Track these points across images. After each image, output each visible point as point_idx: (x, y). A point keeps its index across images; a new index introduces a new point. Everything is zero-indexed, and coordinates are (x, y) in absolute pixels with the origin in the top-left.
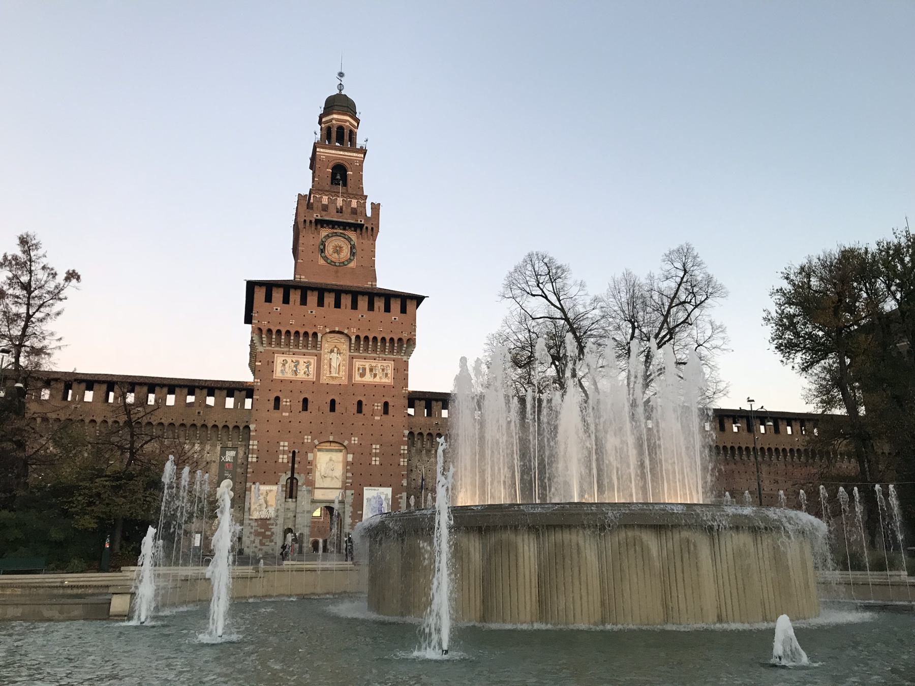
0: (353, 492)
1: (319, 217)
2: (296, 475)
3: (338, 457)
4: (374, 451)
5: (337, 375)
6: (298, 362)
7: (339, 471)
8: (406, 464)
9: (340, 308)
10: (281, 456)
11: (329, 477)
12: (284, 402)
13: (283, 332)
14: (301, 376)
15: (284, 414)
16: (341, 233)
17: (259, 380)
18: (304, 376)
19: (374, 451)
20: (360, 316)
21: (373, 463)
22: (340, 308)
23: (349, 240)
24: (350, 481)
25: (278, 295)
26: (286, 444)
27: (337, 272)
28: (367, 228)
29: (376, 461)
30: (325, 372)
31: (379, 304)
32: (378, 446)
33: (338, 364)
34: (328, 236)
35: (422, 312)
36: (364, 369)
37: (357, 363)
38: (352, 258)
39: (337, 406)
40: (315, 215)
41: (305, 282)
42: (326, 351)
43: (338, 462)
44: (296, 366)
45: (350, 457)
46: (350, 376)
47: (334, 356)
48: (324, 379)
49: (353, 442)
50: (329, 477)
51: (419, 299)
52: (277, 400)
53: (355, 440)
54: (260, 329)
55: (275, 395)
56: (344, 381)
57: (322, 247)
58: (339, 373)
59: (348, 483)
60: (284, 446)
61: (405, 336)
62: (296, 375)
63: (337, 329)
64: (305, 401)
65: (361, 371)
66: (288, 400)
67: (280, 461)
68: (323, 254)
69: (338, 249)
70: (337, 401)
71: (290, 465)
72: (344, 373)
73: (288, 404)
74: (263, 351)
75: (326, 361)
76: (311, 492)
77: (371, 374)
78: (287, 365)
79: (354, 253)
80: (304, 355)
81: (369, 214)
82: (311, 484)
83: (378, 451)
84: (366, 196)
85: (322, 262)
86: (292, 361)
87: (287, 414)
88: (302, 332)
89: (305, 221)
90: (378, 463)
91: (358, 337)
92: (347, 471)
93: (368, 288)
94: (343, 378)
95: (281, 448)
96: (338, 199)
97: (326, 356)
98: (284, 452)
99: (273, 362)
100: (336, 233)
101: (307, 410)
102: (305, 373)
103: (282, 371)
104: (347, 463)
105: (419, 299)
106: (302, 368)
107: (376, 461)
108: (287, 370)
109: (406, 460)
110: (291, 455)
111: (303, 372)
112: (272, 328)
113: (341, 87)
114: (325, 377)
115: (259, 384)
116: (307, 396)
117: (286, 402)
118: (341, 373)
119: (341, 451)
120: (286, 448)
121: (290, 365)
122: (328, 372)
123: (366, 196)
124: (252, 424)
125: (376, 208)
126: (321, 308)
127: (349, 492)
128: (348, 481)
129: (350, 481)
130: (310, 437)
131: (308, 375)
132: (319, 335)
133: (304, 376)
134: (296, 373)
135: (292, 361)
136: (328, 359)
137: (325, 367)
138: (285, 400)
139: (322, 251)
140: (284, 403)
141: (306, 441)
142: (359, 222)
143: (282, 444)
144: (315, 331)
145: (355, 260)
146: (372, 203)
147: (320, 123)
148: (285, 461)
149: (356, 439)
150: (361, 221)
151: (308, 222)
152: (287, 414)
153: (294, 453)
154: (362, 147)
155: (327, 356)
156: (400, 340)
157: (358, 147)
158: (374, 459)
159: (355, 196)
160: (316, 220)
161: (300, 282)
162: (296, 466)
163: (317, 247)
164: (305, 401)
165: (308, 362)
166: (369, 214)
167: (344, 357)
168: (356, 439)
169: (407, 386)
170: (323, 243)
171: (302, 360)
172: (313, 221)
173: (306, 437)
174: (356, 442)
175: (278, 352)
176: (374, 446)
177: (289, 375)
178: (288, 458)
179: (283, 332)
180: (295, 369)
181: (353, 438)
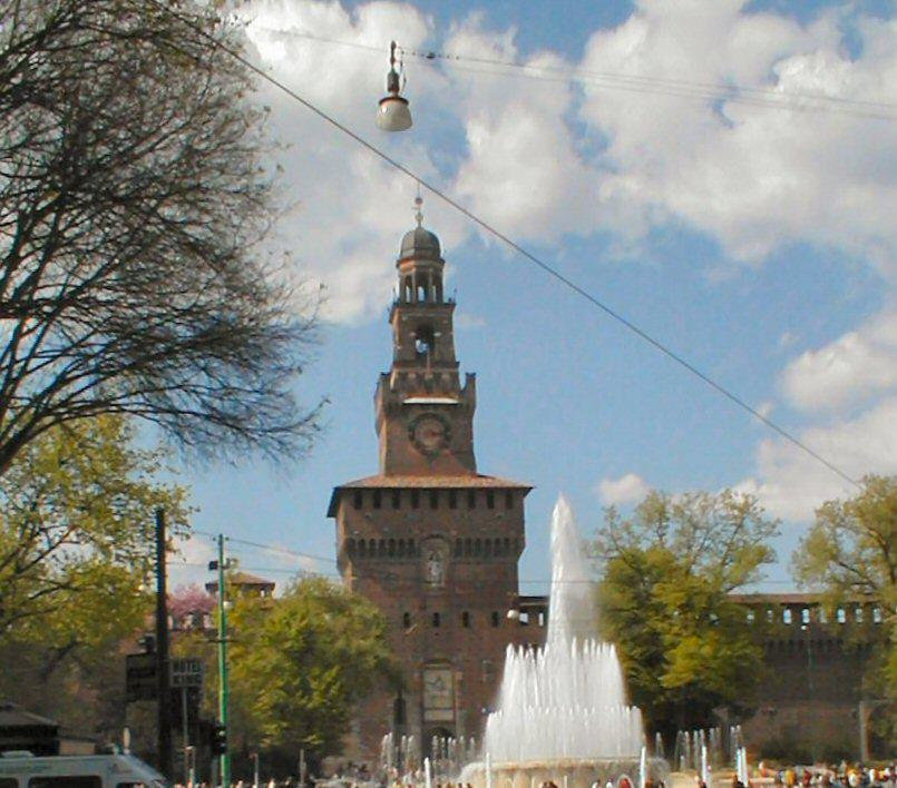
2: (404, 696)
3: (446, 676)
23: (442, 420)
25: (367, 501)
31: (481, 501)
34: (419, 419)
35: (528, 500)
39: (441, 620)
51: (526, 490)
54: (353, 541)
61: (512, 534)
63: (435, 532)
76: (422, 714)
81: (462, 382)
88: (396, 539)
91: (458, 542)
105: (526, 490)
113: (419, 218)
119: (448, 668)
125: (471, 378)
132: (416, 542)
146: (467, 374)
147: (398, 266)
154: (450, 300)
156: (507, 540)
157: (446, 300)
160: (405, 404)
166: (462, 382)
169: (516, 590)
176: (484, 662)
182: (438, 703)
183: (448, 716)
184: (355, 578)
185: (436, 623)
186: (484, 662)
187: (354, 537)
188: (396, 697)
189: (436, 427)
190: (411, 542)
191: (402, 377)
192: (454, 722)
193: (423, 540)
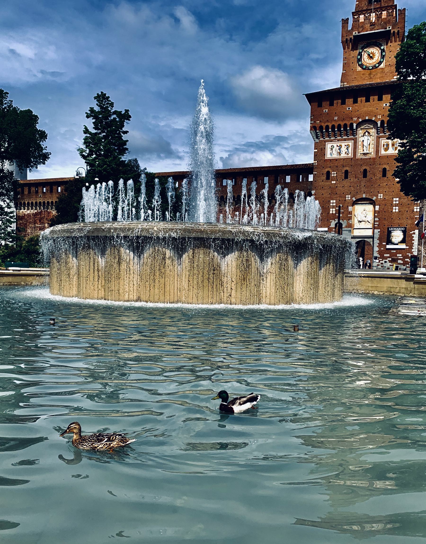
0: (379, 230)
1: (357, 34)
2: (341, 221)
4: (394, 202)
5: (368, 152)
6: (341, 146)
7: (370, 217)
8: (418, 210)
9: (369, 101)
10: (331, 210)
11: (364, 221)
12: (334, 174)
13: (330, 126)
14: (343, 155)
15: (333, 182)
16: (374, 42)
17: (316, 162)
18: (345, 155)
19: (394, 202)
20: (384, 105)
21: (394, 211)
22: (369, 101)
24: (378, 223)
26: (334, 201)
27: (370, 74)
28: (394, 32)
29: (396, 209)
30: (359, 151)
32: (397, 199)
33: (368, 144)
36: (388, 145)
37: (383, 141)
38: (382, 60)
39: (368, 174)
40: (354, 32)
41: (346, 87)
42: (360, 135)
43: (369, 211)
44: (340, 149)
45: (377, 208)
46: (377, 151)
47: (365, 138)
48: (359, 156)
49: (379, 197)
50: (364, 221)
52: (328, 173)
53: (381, 196)
55: (327, 170)
56: (373, 155)
57: (359, 57)
58: (369, 150)
59: (376, 225)
60: (333, 203)
62: (340, 155)
63: (367, 118)
64: (346, 172)
65: (385, 147)
66: (335, 173)
67: (331, 212)
68: (360, 63)
69: (371, 55)
70: (368, 169)
71: (337, 215)
72: (373, 150)
73: (335, 175)
74: (318, 141)
75: (360, 143)
77: (393, 148)
78: (334, 149)
79: (384, 56)
80: (345, 140)
82: (350, 226)
83: (397, 202)
84: (396, 5)
85: (359, 69)
86: (337, 146)
87: (335, 182)
88: (342, 124)
89: (347, 39)
90: (397, 211)
92: (375, 217)
93: (393, 82)
94: (372, 153)
95: (331, 204)
96: (372, 14)
97: (360, 139)
98: (333, 207)
99: (325, 148)
100: (370, 43)
101: (348, 178)
102: (346, 153)
103: (331, 154)
104: (375, 212)
106: (344, 149)
107: (396, 209)
108: (334, 152)
109: (418, 207)
110: (337, 208)
111: (344, 152)
112: (323, 124)
114: (359, 154)
115: (316, 164)
116: (347, 168)
117: (334, 174)
118: (371, 150)
119: (371, 204)
120: (334, 204)
121: (336, 148)
122: (362, 150)
123: (396, 5)
124: (313, 190)
126: (356, 104)
127: (376, 231)
128: (375, 223)
129: (378, 223)
130: (350, 196)
131: (348, 154)
133: (345, 155)
134: (340, 154)
135: (337, 146)
136: (362, 141)
137: (360, 147)
138: (333, 173)
139: (359, 60)
140: (333, 175)
141: (347, 199)
142: (388, 29)
143: (332, 201)
144: (351, 122)
145: (384, 61)
148: (334, 212)
149: (382, 195)
150: (389, 28)
151: (349, 39)
152: (335, 182)
153: (340, 207)
155: (361, 139)
158: (394, 208)
159: (386, 8)
161: (344, 87)
162: (341, 215)
163: (356, 58)
164: (346, 172)
165: (348, 145)
167: (373, 138)
168: (382, 195)
170: (360, 54)
171: (343, 144)
172: (353, 38)
173: (347, 196)
174: (382, 197)
175: (328, 141)
176: (394, 199)
177: (335, 156)
178: (336, 210)
179: (330, 126)
180: (339, 151)
181: (379, 195)
182: (363, 225)
183: (369, 233)
184: (316, 150)
185: (365, 176)
186: (394, 199)
187: (316, 126)
188: (337, 221)
189: (376, 51)
190: (352, 125)
191: (356, 21)
192: (372, 237)
193: (359, 125)
